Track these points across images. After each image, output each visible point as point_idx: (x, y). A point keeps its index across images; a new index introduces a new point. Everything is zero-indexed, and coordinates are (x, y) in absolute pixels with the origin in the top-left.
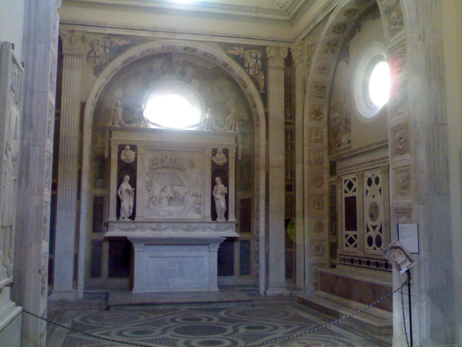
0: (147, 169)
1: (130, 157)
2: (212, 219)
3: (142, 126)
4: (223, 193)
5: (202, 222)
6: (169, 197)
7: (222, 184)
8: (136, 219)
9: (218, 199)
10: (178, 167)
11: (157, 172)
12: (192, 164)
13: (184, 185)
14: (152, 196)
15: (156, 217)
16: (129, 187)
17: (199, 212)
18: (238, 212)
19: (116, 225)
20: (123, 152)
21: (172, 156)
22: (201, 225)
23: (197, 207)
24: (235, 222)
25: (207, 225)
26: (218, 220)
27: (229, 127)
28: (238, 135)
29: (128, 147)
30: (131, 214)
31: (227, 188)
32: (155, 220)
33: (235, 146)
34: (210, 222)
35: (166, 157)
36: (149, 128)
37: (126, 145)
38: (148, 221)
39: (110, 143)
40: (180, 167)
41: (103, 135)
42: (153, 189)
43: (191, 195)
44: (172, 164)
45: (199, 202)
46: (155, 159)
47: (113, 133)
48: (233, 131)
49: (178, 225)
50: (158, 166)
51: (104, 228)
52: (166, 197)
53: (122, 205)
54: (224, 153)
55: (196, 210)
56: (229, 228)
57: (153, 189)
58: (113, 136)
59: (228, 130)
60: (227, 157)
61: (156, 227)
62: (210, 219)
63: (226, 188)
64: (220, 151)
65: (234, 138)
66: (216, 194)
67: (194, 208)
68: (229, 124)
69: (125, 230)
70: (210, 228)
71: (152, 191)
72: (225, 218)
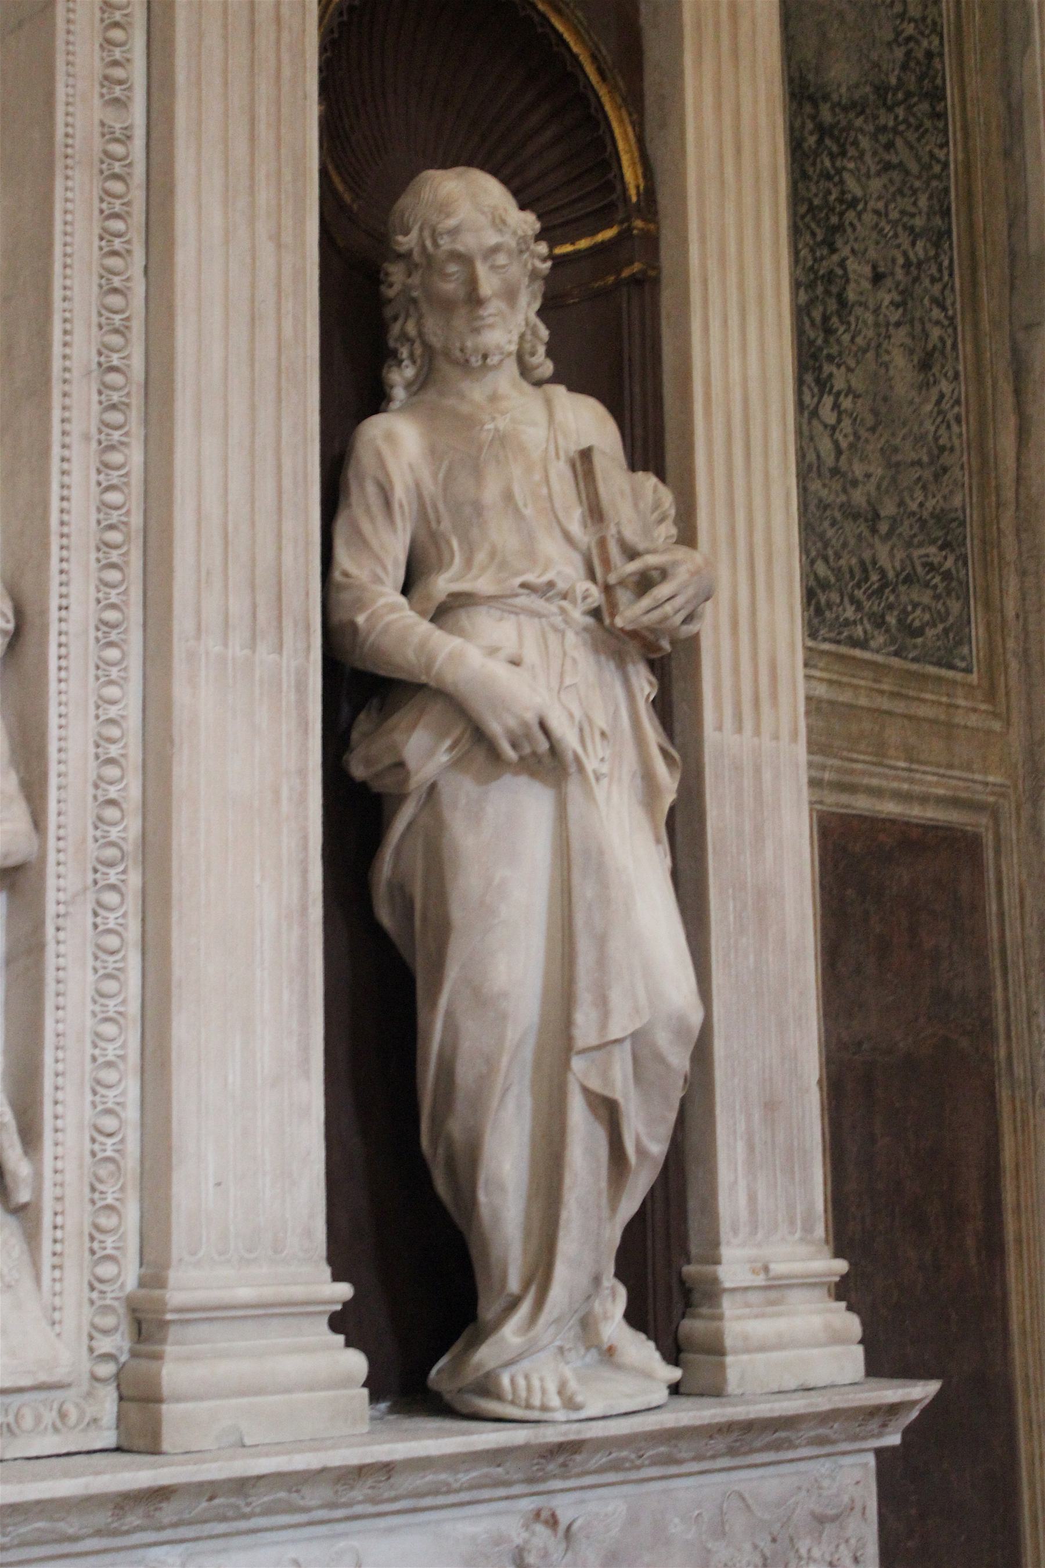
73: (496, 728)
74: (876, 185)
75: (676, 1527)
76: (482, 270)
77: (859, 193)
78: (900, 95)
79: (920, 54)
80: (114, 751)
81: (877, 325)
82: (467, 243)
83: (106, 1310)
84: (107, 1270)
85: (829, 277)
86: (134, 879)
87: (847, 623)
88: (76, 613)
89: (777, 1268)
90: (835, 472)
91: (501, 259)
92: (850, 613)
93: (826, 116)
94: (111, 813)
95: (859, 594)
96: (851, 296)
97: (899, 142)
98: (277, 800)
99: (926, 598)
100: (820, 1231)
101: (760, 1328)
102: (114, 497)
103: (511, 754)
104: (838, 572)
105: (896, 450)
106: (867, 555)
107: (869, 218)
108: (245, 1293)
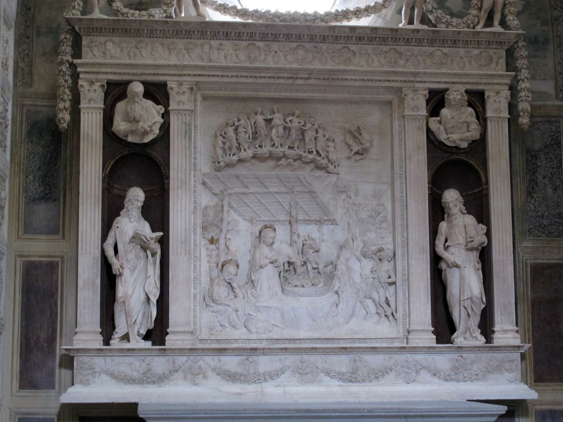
0: (205, 167)
1: (144, 125)
2: (437, 339)
3: (183, 15)
4: (476, 244)
5: (402, 349)
6: (282, 260)
7: (469, 213)
8: (171, 341)
9: (457, 266)
10: (311, 156)
11: (238, 177)
12: (356, 148)
13: (333, 222)
14: (223, 259)
15: (240, 333)
16: (145, 229)
17: (389, 313)
18: (525, 308)
19: (99, 362)
20: (120, 106)
21: (288, 120)
22: (401, 358)
23: (380, 295)
24: (519, 347)
25: (420, 357)
26: (459, 339)
27: (484, 15)
28: (517, 42)
29: (138, 88)
30: (151, 326)
31: (484, 227)
32: (235, 345)
33: (508, 81)
34: (430, 349)
35: (268, 121)
36: (207, 20)
37: (126, 84)
38: (214, 346)
39: (75, 76)
40: (318, 158)
41: (56, 51)
42: (226, 235)
43: (358, 254)
44: (290, 148)
45: (390, 277)
46: (230, 131)
47: (85, 42)
48: (497, 28)
49: (318, 360)
50: (243, 155)
51: (62, 374)
52: (272, 263)
53: (121, 291)
54: (470, 105)
55: (378, 305)
56: (499, 368)
57: (226, 235)
58: (84, 50)
59: (481, 24)
60: (482, 118)
61: (240, 370)
62: (430, 339)
63: (483, 228)
64: (459, 97)
65: (504, 54)
66: (446, 248)
67: (371, 298)
68: (482, 5)
69: (131, 381)
70: (428, 369)
71: (222, 241)
72: (482, 333)
73: (449, 263)
74: (544, 162)
75: (483, 359)
76: (450, 204)
77: (540, 164)
78: (550, 146)
79: (555, 137)
80: (404, 269)
81: (544, 185)
82: (448, 201)
83: (405, 330)
84: (405, 326)
85: (533, 180)
86: (407, 283)
87: (536, 234)
88: (399, 253)
89: (504, 328)
90: (534, 210)
91: (453, 202)
92: (537, 232)
93: (533, 154)
94: (404, 276)
95: (539, 229)
96: (538, 182)
97: (550, 154)
98: (424, 273)
99: (555, 227)
100: (515, 323)
101: (500, 336)
102: (403, 240)
103: (451, 265)
104: (535, 226)
105: (548, 205)
106: (541, 222)
107: (543, 168)
108: (419, 328)
